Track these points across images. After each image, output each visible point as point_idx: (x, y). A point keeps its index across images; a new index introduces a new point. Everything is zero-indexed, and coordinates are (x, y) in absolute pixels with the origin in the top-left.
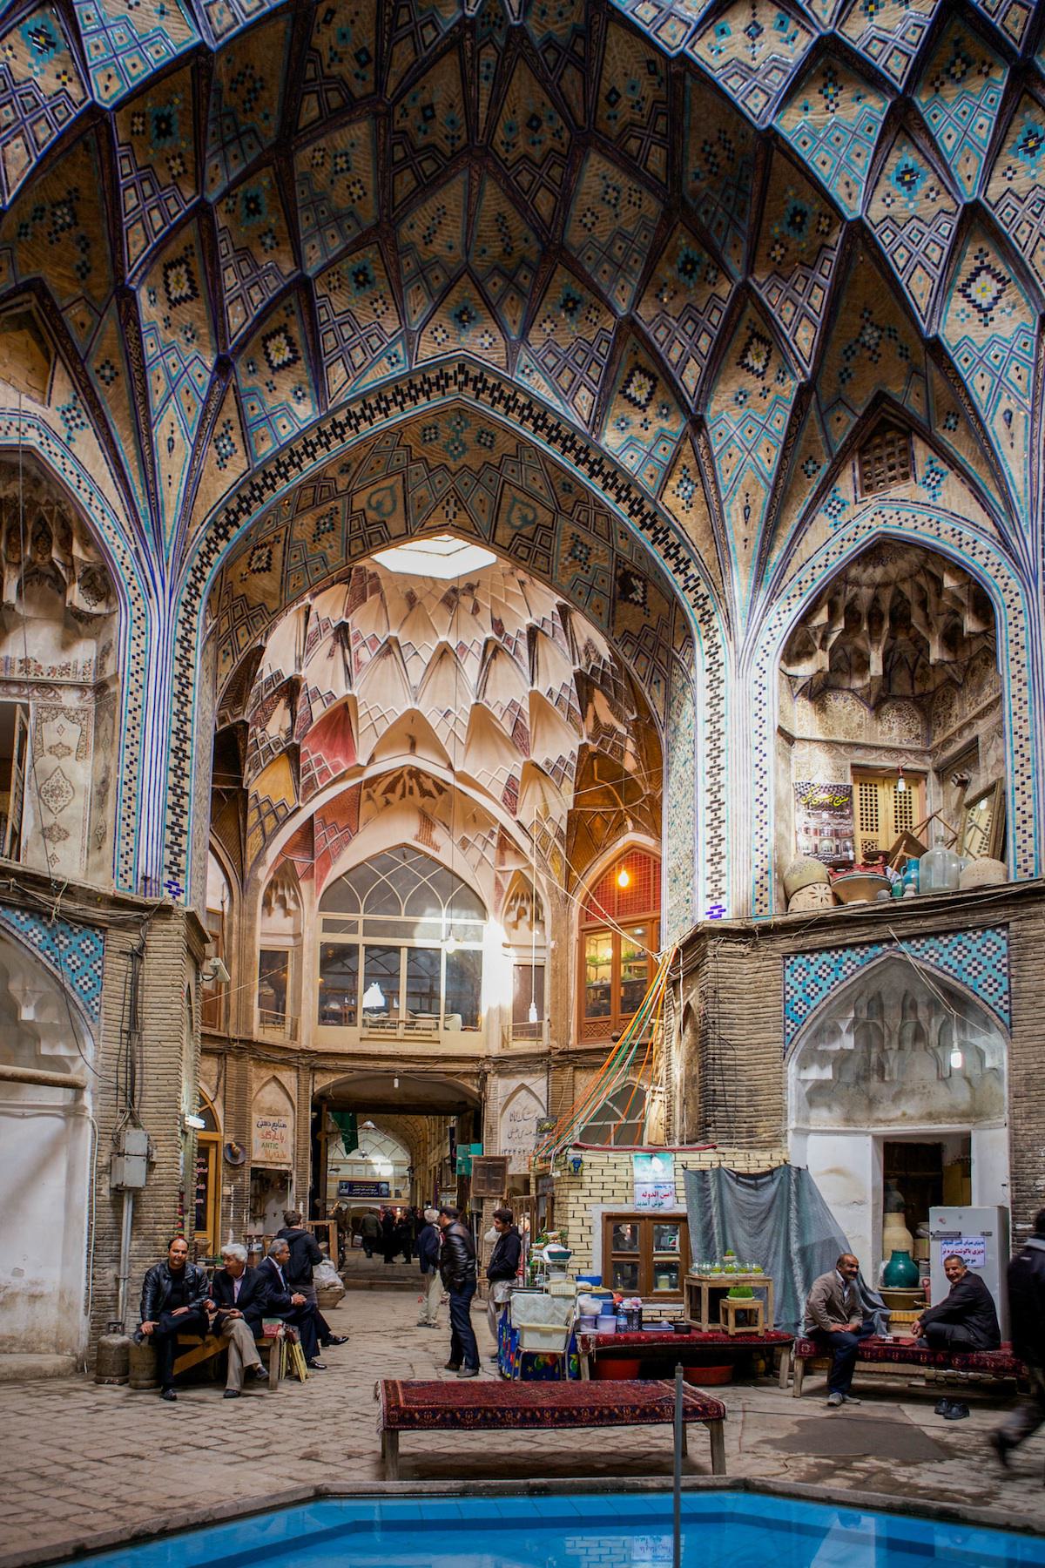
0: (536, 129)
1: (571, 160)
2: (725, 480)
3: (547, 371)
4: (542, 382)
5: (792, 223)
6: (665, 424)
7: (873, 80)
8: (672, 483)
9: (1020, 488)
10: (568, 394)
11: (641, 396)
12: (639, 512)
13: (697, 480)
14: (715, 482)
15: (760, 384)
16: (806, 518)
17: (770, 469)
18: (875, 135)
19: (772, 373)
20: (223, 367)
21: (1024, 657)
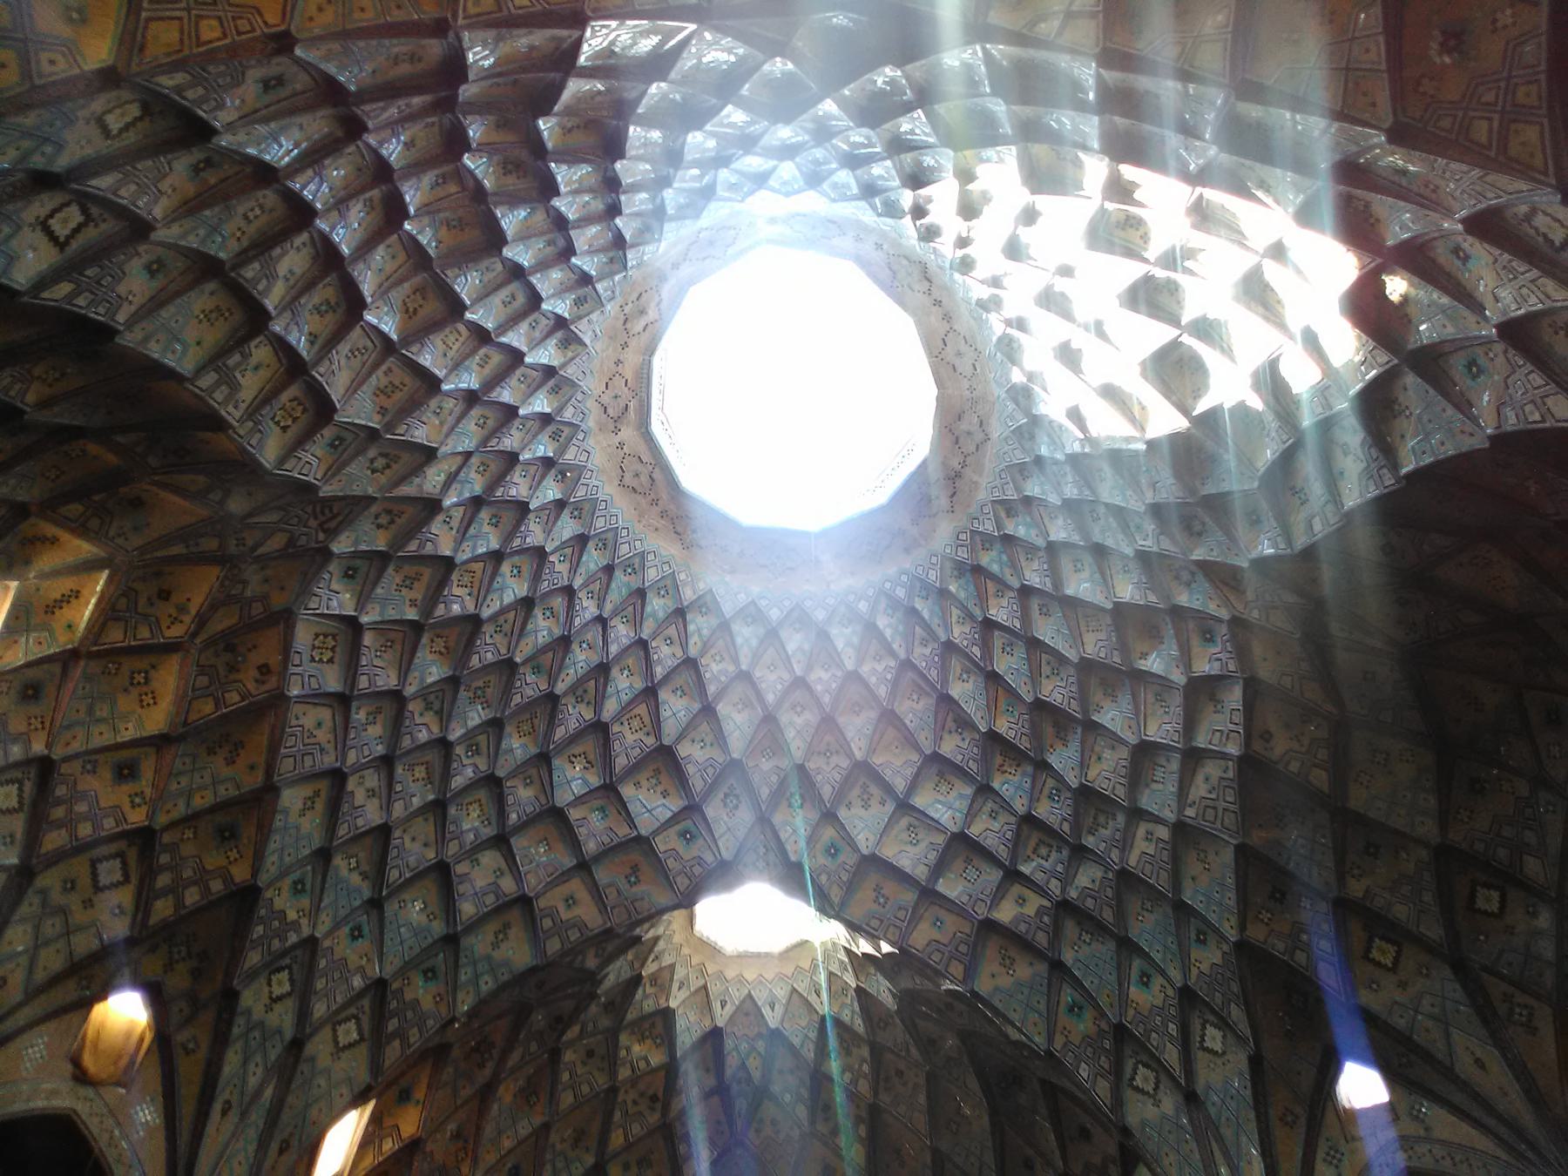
20: (1460, 968)
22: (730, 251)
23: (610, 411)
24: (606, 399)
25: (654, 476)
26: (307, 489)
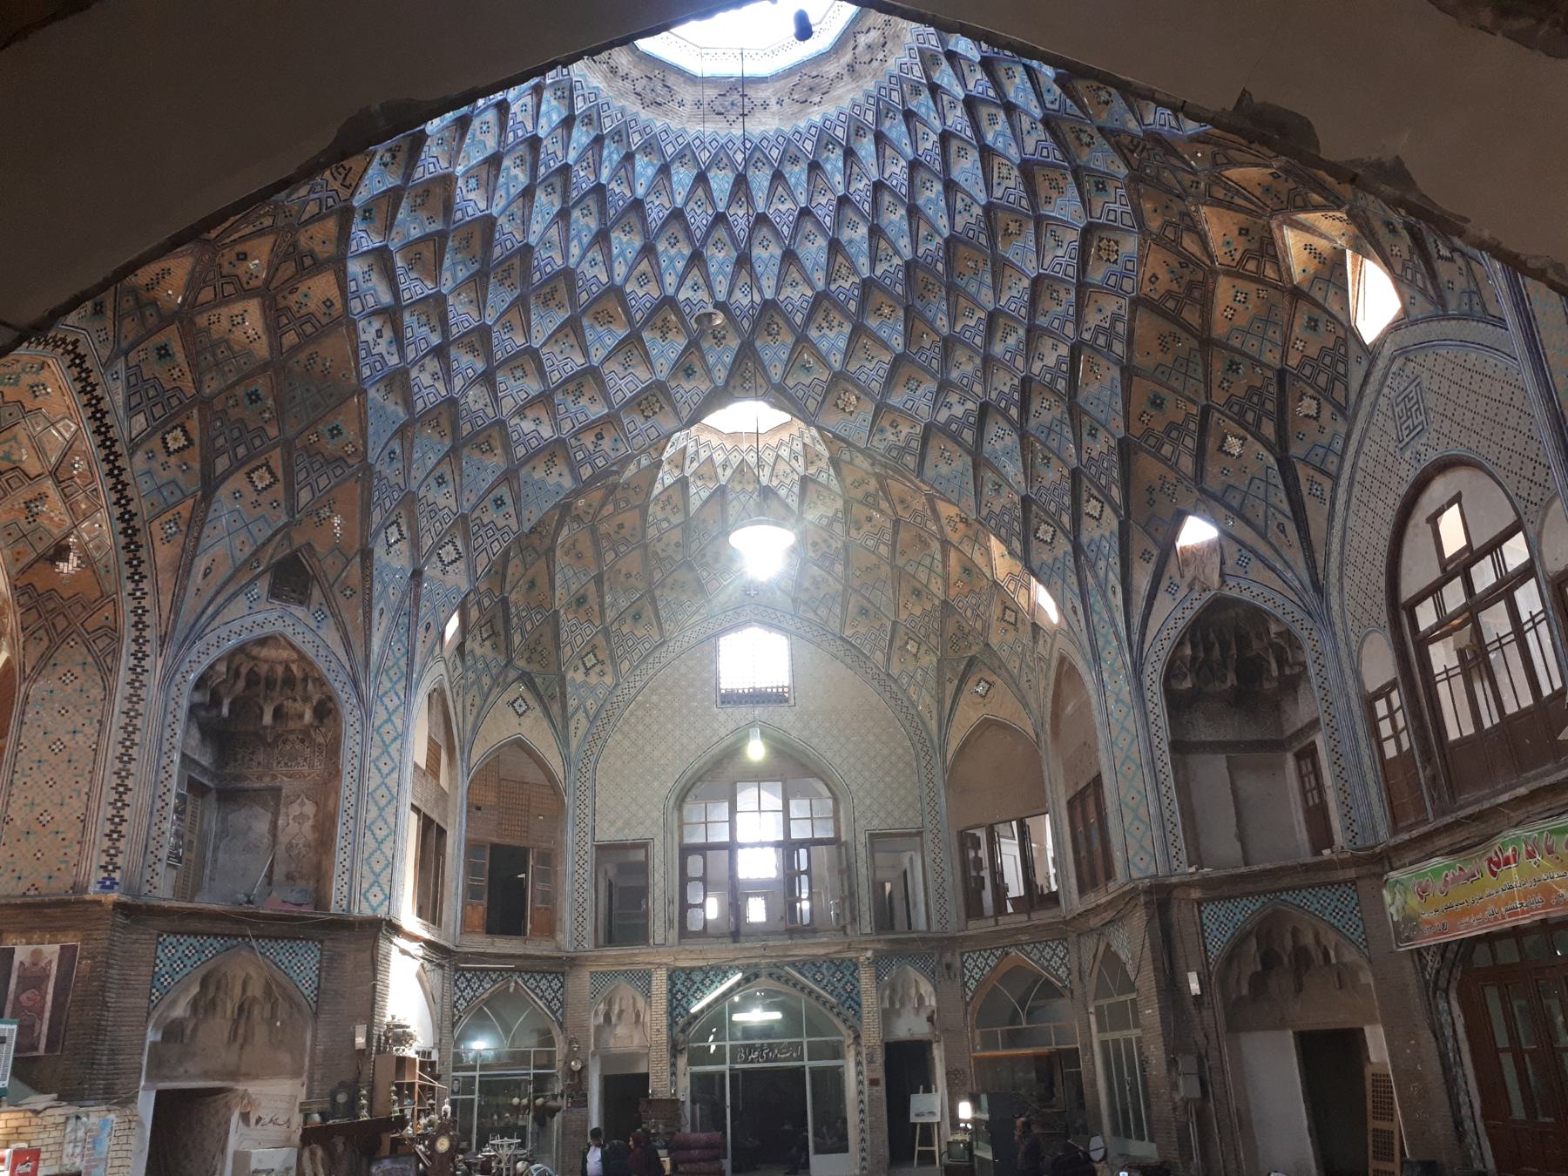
0: (239, 259)
1: (245, 293)
2: (205, 542)
3: (129, 385)
4: (120, 390)
5: (331, 431)
6: (180, 474)
7: (408, 403)
8: (164, 518)
10: (131, 410)
11: (173, 446)
12: (128, 521)
13: (184, 528)
14: (198, 539)
15: (254, 497)
16: (235, 595)
17: (241, 557)
18: (396, 426)
19: (266, 497)
21: (356, 762)
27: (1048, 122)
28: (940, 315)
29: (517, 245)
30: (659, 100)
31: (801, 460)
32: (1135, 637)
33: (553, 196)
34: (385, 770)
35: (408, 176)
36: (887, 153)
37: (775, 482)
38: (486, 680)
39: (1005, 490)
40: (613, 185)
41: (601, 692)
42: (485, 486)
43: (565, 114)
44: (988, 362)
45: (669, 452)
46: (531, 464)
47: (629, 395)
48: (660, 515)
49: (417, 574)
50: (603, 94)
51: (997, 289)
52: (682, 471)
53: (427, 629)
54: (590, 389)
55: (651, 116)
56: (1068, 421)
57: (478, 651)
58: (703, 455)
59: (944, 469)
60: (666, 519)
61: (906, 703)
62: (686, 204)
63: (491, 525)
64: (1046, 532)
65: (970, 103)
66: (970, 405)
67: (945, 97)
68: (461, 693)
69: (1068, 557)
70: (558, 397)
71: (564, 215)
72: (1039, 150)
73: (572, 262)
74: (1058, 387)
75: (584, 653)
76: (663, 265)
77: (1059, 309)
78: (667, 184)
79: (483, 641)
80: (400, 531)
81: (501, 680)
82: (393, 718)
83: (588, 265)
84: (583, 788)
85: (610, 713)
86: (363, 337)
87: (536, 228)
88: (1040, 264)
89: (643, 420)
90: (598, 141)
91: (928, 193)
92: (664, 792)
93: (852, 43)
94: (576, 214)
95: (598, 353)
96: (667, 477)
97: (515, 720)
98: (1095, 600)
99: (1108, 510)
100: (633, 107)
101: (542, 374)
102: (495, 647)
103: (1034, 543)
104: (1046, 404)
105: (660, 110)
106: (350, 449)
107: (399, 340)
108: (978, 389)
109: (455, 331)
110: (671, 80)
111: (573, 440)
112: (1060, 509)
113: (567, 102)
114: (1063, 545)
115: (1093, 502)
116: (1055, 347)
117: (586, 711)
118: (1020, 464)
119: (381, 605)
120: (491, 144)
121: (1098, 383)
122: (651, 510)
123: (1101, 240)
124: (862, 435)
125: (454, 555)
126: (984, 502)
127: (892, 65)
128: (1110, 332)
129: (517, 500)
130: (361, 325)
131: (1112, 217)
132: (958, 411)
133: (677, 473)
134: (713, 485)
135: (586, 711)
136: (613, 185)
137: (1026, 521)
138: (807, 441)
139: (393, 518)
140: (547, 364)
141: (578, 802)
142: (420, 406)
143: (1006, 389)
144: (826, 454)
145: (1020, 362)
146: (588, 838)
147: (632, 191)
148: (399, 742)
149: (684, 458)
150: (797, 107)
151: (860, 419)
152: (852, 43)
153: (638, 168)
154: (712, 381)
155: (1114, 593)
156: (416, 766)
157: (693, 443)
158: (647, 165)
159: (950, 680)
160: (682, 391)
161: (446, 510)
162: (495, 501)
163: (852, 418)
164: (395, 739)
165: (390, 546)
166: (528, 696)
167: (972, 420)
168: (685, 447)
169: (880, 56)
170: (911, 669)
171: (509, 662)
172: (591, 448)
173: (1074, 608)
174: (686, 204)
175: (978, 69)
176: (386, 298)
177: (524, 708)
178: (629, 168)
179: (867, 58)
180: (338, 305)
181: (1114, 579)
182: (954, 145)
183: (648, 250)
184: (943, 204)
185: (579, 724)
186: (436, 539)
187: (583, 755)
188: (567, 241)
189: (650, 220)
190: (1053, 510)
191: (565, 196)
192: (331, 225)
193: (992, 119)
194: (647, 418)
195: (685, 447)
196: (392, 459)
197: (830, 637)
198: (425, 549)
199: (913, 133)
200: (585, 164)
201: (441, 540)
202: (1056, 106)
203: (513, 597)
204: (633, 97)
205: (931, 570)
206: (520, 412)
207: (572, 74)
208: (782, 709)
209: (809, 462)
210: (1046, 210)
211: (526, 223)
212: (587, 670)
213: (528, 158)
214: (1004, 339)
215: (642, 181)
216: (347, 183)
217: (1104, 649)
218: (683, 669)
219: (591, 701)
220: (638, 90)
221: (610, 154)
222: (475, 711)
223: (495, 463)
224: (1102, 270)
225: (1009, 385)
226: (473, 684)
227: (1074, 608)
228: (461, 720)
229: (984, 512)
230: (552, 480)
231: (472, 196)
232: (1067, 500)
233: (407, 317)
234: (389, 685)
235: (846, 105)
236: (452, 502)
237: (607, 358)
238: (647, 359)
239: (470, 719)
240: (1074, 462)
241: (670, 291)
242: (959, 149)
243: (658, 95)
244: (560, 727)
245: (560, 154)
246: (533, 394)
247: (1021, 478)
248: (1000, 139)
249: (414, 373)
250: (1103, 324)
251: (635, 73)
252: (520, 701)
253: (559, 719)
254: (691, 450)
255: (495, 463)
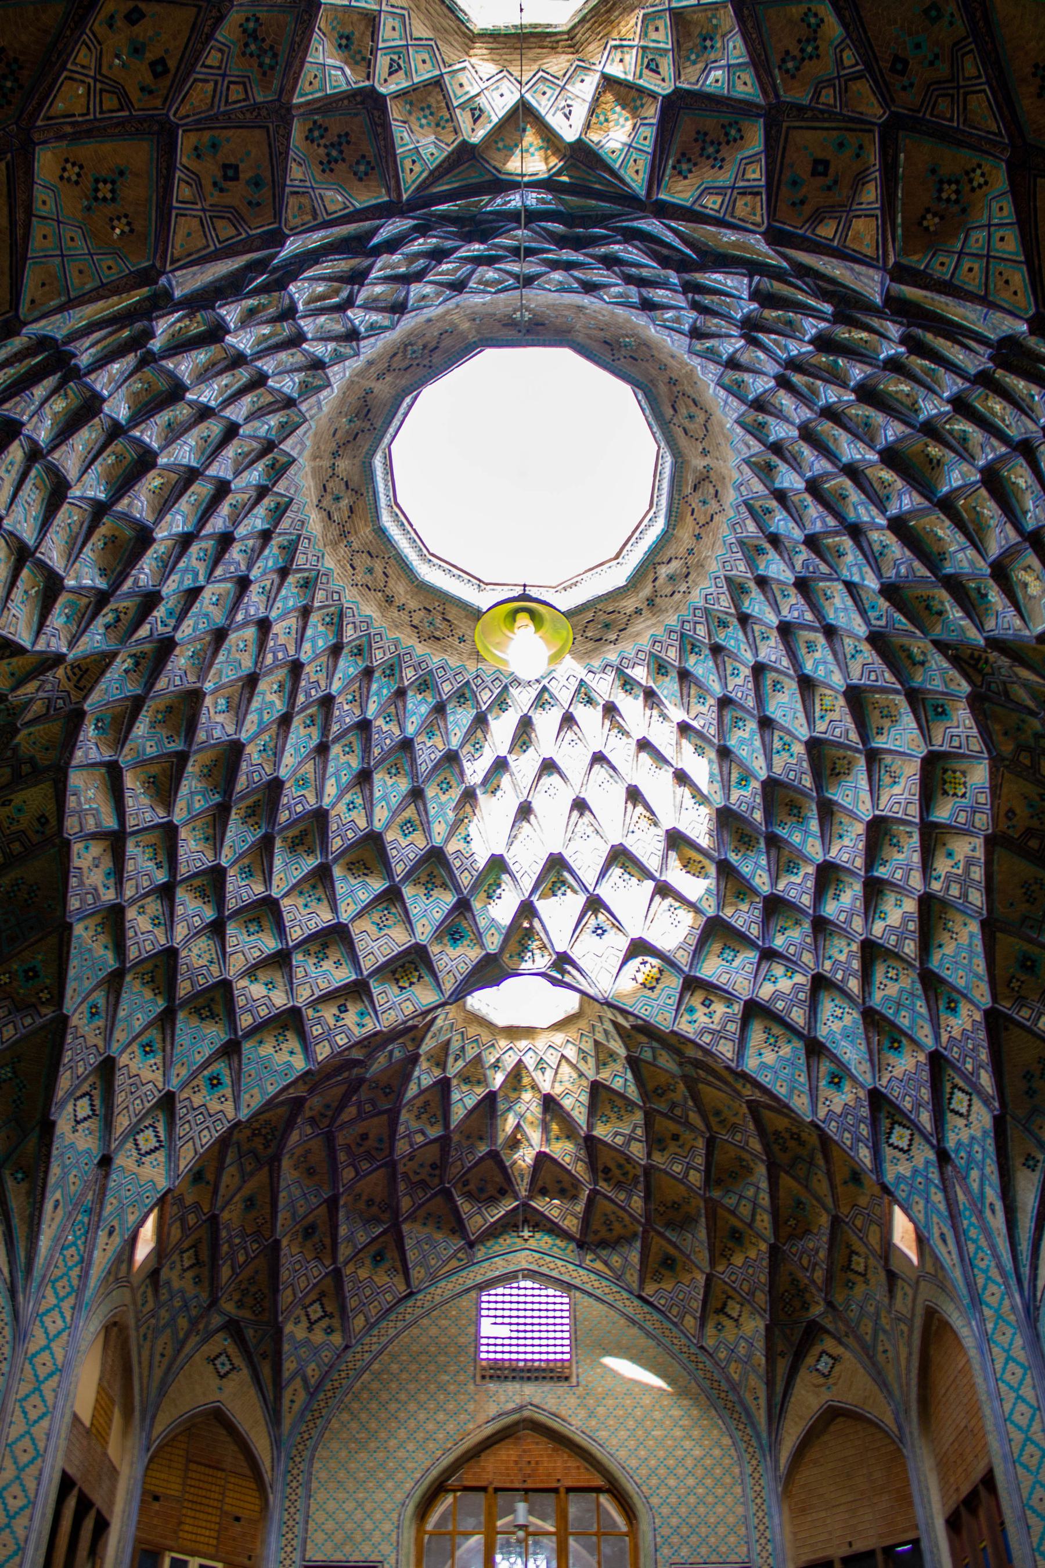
5: (26, 972)
7: (119, 946)
9: (41, 1261)
18: (102, 975)
22: (590, 615)
23: (712, 491)
24: (714, 506)
25: (672, 412)
26: (976, 702)
27: (876, 639)
28: (759, 872)
29: (266, 778)
30: (438, 634)
31: (591, 1061)
32: (1026, 1271)
33: (312, 728)
34: (33, 1415)
35: (150, 685)
36: (692, 692)
37: (558, 1090)
38: (183, 1323)
39: (847, 1086)
40: (380, 722)
41: (326, 1355)
42: (199, 1059)
43: (332, 640)
44: (821, 926)
45: (428, 1045)
46: (257, 1038)
47: (383, 960)
48: (415, 1125)
49: (106, 1162)
50: (376, 624)
51: (826, 837)
52: (444, 1070)
53: (111, 1233)
54: (335, 953)
55: (428, 651)
56: (920, 992)
57: (176, 1284)
58: (471, 1053)
59: (769, 1057)
60: (423, 1132)
61: (724, 1386)
62: (462, 746)
63: (202, 1109)
64: (901, 1137)
65: (786, 630)
66: (799, 978)
67: (756, 627)
68: (149, 1336)
69: (931, 1169)
70: (297, 958)
71: (322, 749)
72: (866, 674)
73: (326, 802)
74: (906, 950)
75: (307, 1301)
76: (432, 812)
77: (901, 856)
78: (442, 724)
79: (184, 1270)
80: (92, 1105)
81: (201, 1326)
82: (53, 1345)
83: (345, 808)
84: (294, 1484)
85: (336, 1384)
86: (76, 862)
87: (289, 760)
88: (875, 802)
89: (397, 990)
90: (368, 673)
91: (740, 733)
92: (400, 1496)
93: (651, 577)
94: (336, 750)
95: (349, 909)
96: (425, 1076)
97: (215, 1382)
98: (968, 1221)
99: (977, 1105)
100: (409, 640)
101: (280, 929)
102: (197, 1280)
103: (888, 1152)
104: (892, 973)
105: (437, 645)
106: (45, 996)
107: (118, 873)
108: (807, 958)
109: (183, 870)
110: (452, 613)
111: (310, 1012)
112: (918, 1105)
113: (334, 628)
114: (924, 1154)
115: (959, 1095)
116: (898, 904)
117: (305, 1380)
118: (863, 1048)
119: (58, 1195)
120: (247, 663)
121: (954, 944)
122: (404, 1116)
123: (945, 771)
124: (667, 1015)
125: (153, 1143)
126: (821, 1100)
127: (697, 598)
128: (965, 881)
129: (236, 1083)
130: (77, 847)
131: (956, 744)
132: (785, 985)
133: (437, 1073)
134: (481, 1091)
135: (305, 1380)
136: (380, 722)
137: (874, 1123)
138: (600, 1037)
139: (86, 1087)
140: (287, 917)
141: (287, 1504)
142: (133, 953)
143: (843, 958)
144: (622, 1052)
145: (858, 924)
146: (296, 1556)
147: (402, 729)
148: (56, 1378)
149: (447, 1055)
150: (590, 645)
151: (665, 994)
152: (651, 577)
153: (410, 706)
154: (482, 946)
155: (993, 1211)
156: (76, 1418)
157: (459, 1037)
158: (420, 703)
159: (782, 1354)
160: (446, 958)
161: (150, 1086)
162: (211, 1079)
163: (653, 995)
164: (51, 1375)
165: (78, 1122)
166: (232, 1350)
167: (802, 996)
168: (449, 1041)
169: (683, 588)
170: (731, 1338)
171: (214, 1302)
172: (331, 1021)
173: (942, 1235)
174: (462, 746)
175: (793, 591)
176: (110, 823)
177: (228, 1367)
178: (400, 704)
179: (668, 590)
180: (53, 822)
181: (992, 1195)
182: (770, 677)
183: (416, 794)
184: (758, 744)
185: (294, 1397)
186: (134, 1120)
187: (298, 1439)
188: (323, 779)
189: (419, 761)
190: (909, 1106)
191: (325, 729)
192: (55, 728)
193: (811, 647)
194: (402, 988)
195: (449, 1041)
196: (93, 1015)
197: (625, 1295)
198: (119, 1130)
199: (721, 669)
200: (350, 697)
201: (140, 1121)
202: (883, 623)
203: (225, 1216)
204: (409, 629)
205: (755, 1205)
206: (251, 972)
207: (343, 600)
208: (561, 1388)
209: (600, 1064)
210: (879, 742)
211: (277, 754)
212: (312, 1323)
213: (288, 685)
214: (836, 897)
215: (414, 719)
216: (81, 685)
217: (985, 1288)
218: (434, 1331)
219: (313, 1365)
220: (415, 622)
221: (380, 688)
222: (166, 1361)
223: (214, 1034)
224: (949, 806)
225: (846, 951)
226: (165, 1326)
227: (942, 1235)
228: (146, 1373)
229: (822, 1113)
230: (283, 1057)
231: (219, 718)
232: (925, 1094)
233: (131, 848)
234: (54, 1301)
235: (645, 641)
236: (158, 1076)
237: (359, 915)
238: (407, 920)
239: (158, 1373)
240: (929, 1043)
241: (438, 841)
242: (775, 683)
243: (437, 628)
244: (270, 1397)
245: (323, 684)
246: (268, 952)
247: (866, 1066)
248: (821, 667)
249: (131, 913)
250: (955, 871)
251: (412, 604)
252: (223, 1358)
253: (271, 1387)
254: (455, 1045)
255: (214, 1034)
